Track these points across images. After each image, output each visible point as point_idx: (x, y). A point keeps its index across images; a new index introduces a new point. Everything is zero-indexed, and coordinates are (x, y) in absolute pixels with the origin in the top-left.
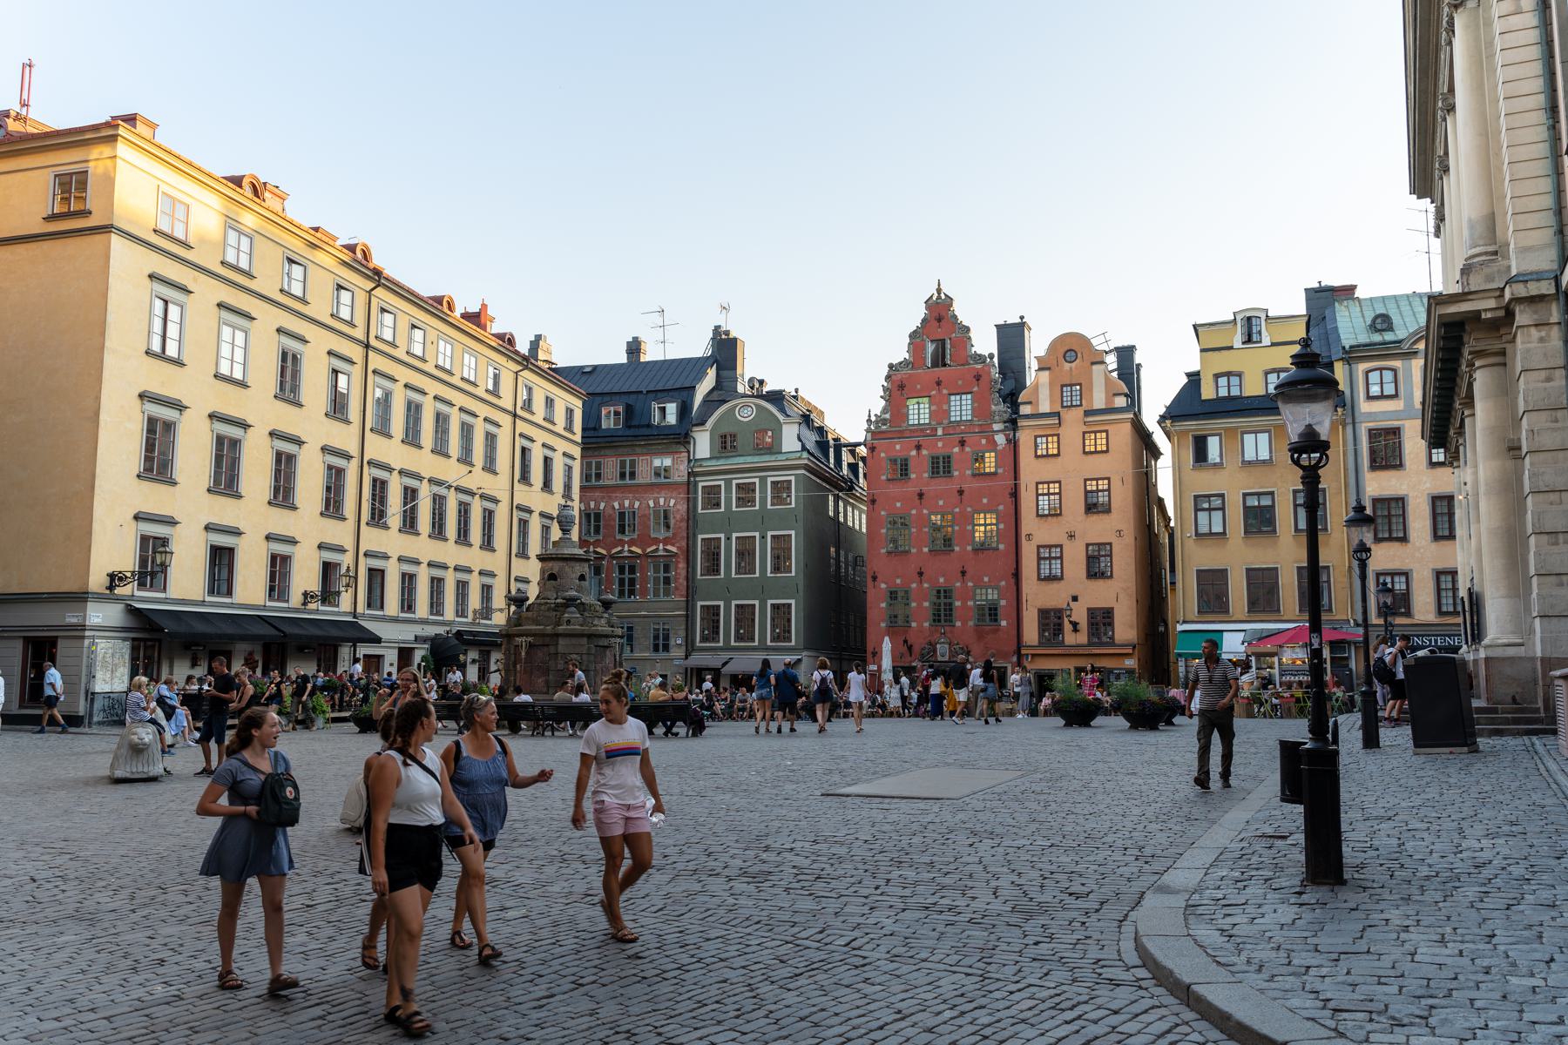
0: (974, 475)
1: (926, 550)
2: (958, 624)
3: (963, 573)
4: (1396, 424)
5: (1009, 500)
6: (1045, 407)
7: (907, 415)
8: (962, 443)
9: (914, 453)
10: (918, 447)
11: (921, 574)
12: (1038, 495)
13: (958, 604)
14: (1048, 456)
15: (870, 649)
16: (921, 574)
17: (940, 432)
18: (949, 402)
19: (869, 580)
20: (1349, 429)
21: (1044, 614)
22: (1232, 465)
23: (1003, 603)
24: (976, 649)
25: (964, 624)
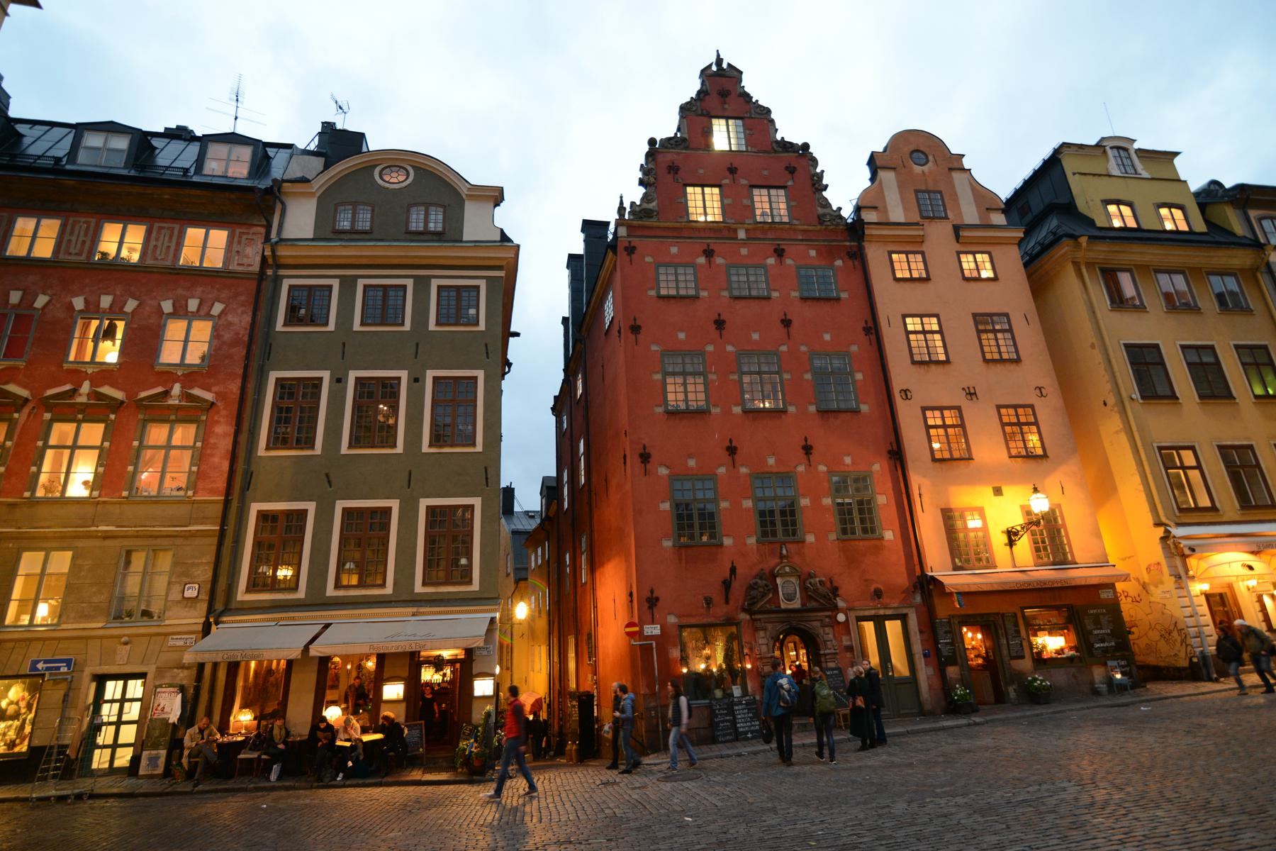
0: (804, 299)
1: (737, 410)
2: (810, 538)
3: (808, 449)
6: (897, 215)
8: (779, 253)
10: (709, 253)
11: (732, 450)
14: (912, 280)
16: (732, 450)
17: (742, 235)
19: (634, 461)
22: (1155, 305)
23: (881, 500)
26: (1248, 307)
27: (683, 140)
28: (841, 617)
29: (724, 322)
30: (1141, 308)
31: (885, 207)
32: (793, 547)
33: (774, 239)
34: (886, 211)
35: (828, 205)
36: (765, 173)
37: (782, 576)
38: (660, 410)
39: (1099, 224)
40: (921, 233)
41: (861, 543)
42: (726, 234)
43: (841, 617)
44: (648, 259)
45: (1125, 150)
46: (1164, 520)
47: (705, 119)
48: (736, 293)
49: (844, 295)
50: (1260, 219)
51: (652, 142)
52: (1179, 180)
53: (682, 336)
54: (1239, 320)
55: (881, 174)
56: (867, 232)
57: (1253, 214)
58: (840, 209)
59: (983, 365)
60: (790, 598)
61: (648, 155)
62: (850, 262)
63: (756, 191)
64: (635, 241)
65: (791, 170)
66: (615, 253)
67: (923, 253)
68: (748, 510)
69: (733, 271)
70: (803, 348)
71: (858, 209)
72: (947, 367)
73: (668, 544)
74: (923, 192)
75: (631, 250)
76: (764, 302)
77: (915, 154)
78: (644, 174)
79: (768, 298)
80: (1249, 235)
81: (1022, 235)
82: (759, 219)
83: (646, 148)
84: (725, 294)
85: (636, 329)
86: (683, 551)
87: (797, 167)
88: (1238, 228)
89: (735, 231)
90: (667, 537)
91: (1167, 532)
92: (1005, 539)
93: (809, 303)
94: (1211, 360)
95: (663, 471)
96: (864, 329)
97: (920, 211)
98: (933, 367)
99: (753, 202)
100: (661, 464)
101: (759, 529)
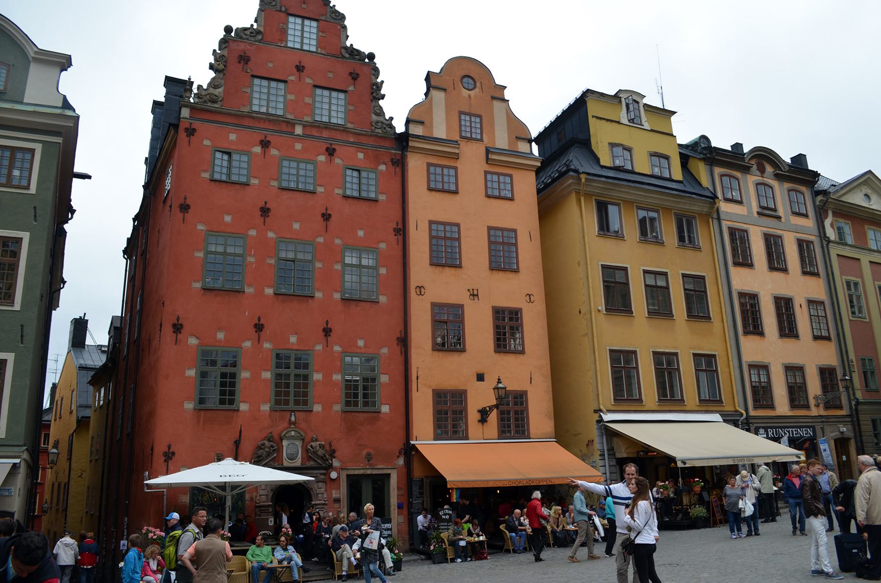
1: (269, 291)
2: (317, 408)
3: (327, 332)
4: (745, 227)
5: (392, 238)
6: (440, 131)
7: (251, 98)
9: (258, 149)
11: (259, 328)
12: (431, 237)
13: (317, 377)
15: (160, 448)
16: (259, 328)
17: (299, 130)
18: (313, 96)
19: (168, 329)
20: (715, 222)
21: (439, 396)
23: (384, 379)
24: (344, 449)
25: (325, 409)
26: (698, 245)
27: (258, 32)
28: (334, 475)
29: (269, 209)
30: (618, 236)
31: (432, 123)
32: (301, 415)
33: (329, 140)
34: (431, 127)
35: (381, 113)
36: (330, 75)
37: (288, 438)
38: (198, 285)
39: (602, 163)
40: (457, 151)
41: (361, 415)
42: (284, 127)
43: (334, 475)
44: (207, 142)
45: (637, 103)
46: (602, 407)
47: (283, 15)
48: (285, 184)
49: (382, 197)
50: (722, 176)
51: (228, 29)
52: (672, 135)
53: (228, 219)
54: (690, 254)
55: (433, 92)
56: (411, 144)
57: (718, 171)
58: (391, 119)
59: (488, 270)
60: (292, 458)
61: (223, 42)
62: (392, 169)
63: (319, 91)
64: (196, 124)
65: (354, 77)
66: (177, 131)
67: (456, 168)
68: (265, 380)
69: (286, 163)
70: (338, 241)
71: (408, 122)
72: (458, 270)
73: (189, 406)
74: (466, 114)
75: (191, 132)
76: (309, 195)
77: (465, 80)
78: (216, 60)
79: (313, 193)
80: (711, 189)
81: (539, 164)
82: (318, 118)
83: (222, 34)
84: (275, 183)
85: (185, 208)
86: (202, 413)
87: (360, 73)
88: (705, 181)
89: (293, 125)
90: (189, 399)
91: (601, 416)
92: (478, 416)
93: (350, 201)
94: (663, 284)
95: (193, 341)
96: (395, 230)
97: (461, 131)
98: (447, 269)
99: (314, 101)
100: (192, 335)
101: (273, 398)
